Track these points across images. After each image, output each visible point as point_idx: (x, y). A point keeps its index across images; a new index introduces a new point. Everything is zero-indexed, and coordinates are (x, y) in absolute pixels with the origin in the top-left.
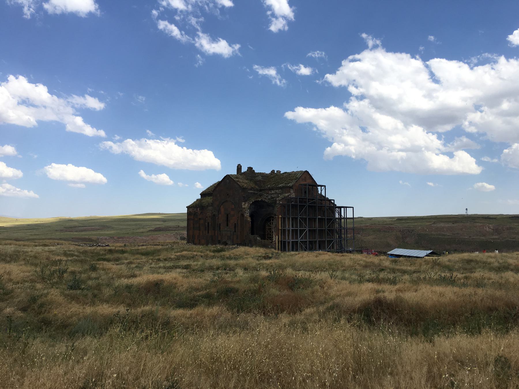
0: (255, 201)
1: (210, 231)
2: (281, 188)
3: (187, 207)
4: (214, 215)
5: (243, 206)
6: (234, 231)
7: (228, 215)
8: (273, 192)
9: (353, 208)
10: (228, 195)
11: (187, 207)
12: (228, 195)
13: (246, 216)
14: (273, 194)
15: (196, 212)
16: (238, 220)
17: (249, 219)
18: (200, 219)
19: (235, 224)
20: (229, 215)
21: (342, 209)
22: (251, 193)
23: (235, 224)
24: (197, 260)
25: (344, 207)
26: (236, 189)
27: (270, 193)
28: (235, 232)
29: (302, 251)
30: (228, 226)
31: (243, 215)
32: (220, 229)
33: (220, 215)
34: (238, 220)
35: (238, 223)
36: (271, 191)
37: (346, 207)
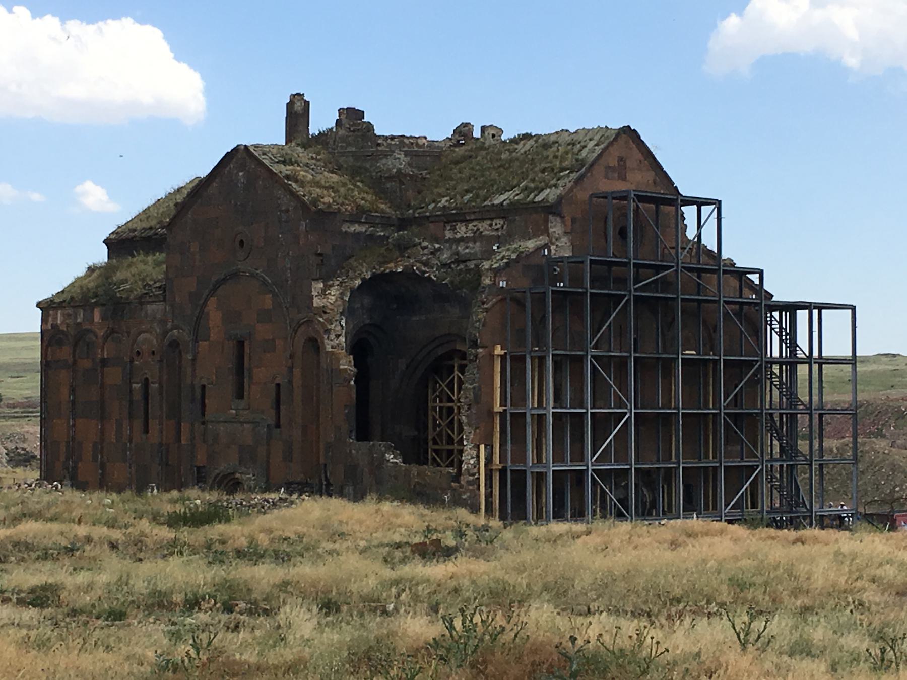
0: (374, 277)
1: (154, 424)
2: (502, 212)
3: (39, 305)
4: (175, 344)
5: (317, 302)
6: (271, 421)
7: (241, 344)
8: (462, 230)
9: (853, 309)
10: (242, 242)
11: (39, 305)
12: (242, 242)
13: (329, 348)
14: (462, 239)
15: (86, 327)
16: (291, 369)
17: (346, 364)
18: (104, 362)
19: (278, 385)
20: (246, 344)
21: (802, 316)
22: (357, 235)
23: (278, 385)
24: (93, 564)
25: (807, 306)
26: (284, 217)
27: (448, 235)
28: (278, 425)
29: (604, 517)
30: (240, 395)
31: (314, 344)
32: (203, 414)
33: (203, 344)
34: (291, 369)
35: (290, 382)
36: (453, 229)
37: (821, 307)
